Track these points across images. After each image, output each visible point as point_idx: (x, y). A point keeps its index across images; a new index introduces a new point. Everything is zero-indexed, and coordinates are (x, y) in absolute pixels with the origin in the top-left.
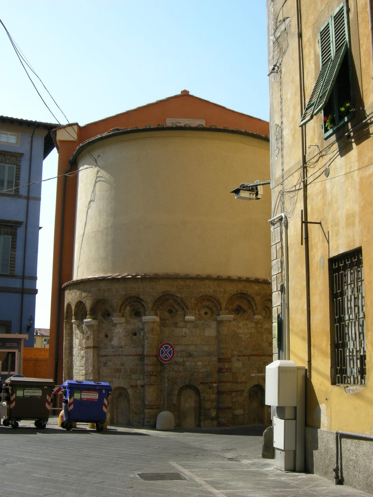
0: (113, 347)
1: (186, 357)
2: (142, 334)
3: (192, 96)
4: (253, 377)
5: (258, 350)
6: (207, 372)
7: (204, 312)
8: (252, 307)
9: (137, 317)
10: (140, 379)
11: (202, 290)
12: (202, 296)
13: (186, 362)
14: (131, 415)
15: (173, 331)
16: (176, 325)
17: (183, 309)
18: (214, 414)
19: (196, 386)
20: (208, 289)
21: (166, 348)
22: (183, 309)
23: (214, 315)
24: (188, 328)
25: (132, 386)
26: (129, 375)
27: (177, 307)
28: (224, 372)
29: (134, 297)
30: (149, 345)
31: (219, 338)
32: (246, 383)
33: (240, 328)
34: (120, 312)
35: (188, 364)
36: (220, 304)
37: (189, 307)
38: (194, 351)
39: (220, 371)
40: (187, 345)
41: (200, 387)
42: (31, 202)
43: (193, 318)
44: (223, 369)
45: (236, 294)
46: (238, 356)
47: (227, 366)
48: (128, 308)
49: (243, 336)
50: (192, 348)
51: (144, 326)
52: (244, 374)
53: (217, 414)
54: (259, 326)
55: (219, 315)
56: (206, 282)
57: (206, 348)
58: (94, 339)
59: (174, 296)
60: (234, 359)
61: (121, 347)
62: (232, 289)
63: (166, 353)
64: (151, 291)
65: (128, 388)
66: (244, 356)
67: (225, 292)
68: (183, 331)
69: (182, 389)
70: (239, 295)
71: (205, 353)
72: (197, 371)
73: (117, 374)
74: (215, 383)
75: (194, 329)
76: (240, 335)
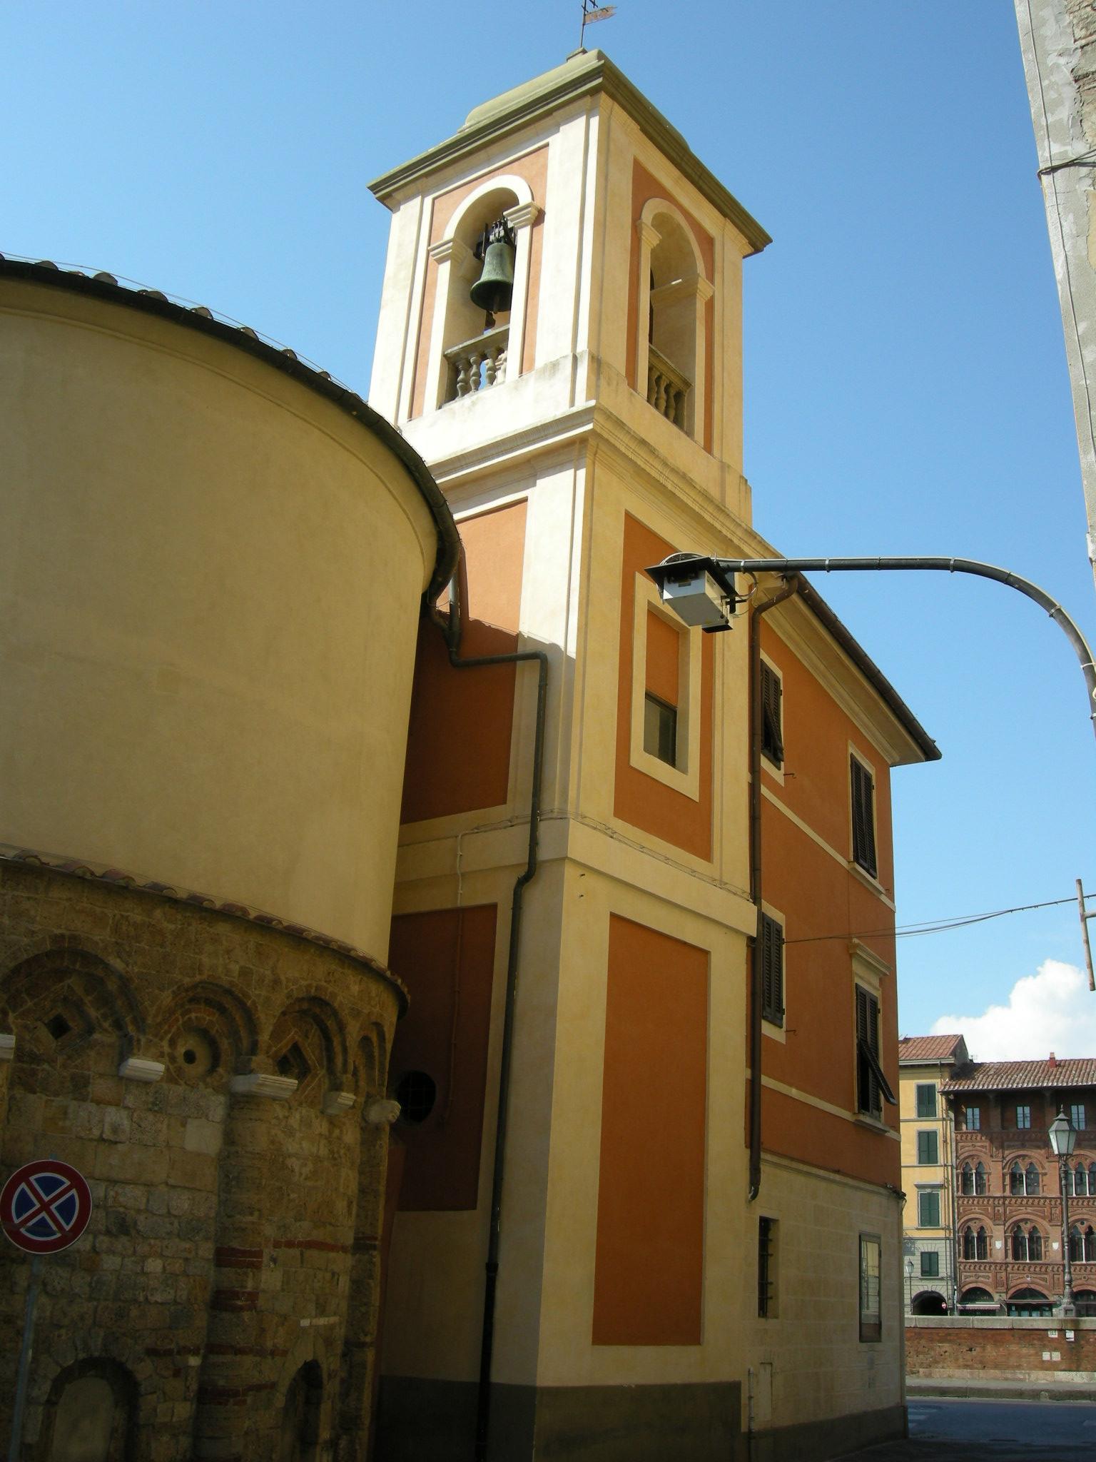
1: (108, 1232)
4: (304, 1329)
6: (176, 1302)
7: (183, 1050)
8: (331, 1060)
11: (205, 960)
12: (195, 986)
13: (104, 1256)
15: (66, 1113)
16: (79, 1087)
17: (118, 1025)
19: (129, 1366)
20: (226, 958)
21: (49, 1185)
22: (118, 1025)
23: (220, 1070)
24: (127, 1108)
27: (93, 1013)
28: (241, 1308)
31: (231, 1165)
32: (285, 1353)
33: (290, 1133)
35: (110, 1263)
36: (253, 1028)
37: (149, 1021)
38: (139, 1211)
39: (222, 1301)
40: (114, 1182)
41: (144, 1370)
43: (159, 1067)
44: (236, 1295)
46: (277, 1245)
47: (250, 1285)
50: (132, 1197)
52: (285, 1317)
55: (242, 1069)
56: (222, 928)
57: (182, 1203)
62: (298, 973)
63: (45, 1207)
66: (290, 1244)
67: (276, 982)
68: (108, 1119)
69: (66, 1376)
70: (305, 1006)
71: (176, 1224)
72: (141, 1299)
74: (195, 1352)
75: (151, 1117)
76: (289, 1162)
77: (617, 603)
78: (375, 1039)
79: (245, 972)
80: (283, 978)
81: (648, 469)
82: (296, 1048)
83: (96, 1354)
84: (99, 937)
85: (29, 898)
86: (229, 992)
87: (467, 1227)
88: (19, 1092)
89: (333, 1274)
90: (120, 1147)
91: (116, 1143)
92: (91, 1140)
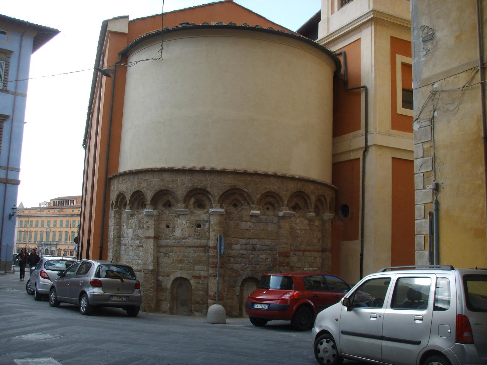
0: (175, 239)
2: (207, 226)
3: (236, 4)
5: (310, 245)
7: (266, 208)
9: (201, 209)
10: (203, 271)
12: (267, 192)
20: (274, 186)
24: (253, 222)
25: (195, 277)
26: (192, 266)
29: (200, 189)
33: (297, 224)
42: (19, 98)
43: (259, 212)
45: (296, 192)
48: (192, 200)
49: (299, 231)
51: (209, 218)
54: (312, 223)
58: (154, 229)
59: (241, 190)
60: (292, 254)
61: (184, 238)
64: (219, 184)
65: (191, 279)
66: (299, 251)
73: (180, 265)
76: (297, 231)
77: (389, 66)
78: (323, 199)
79: (278, 188)
81: (396, 22)
82: (296, 204)
83: (250, 276)
85: (223, 178)
86: (275, 193)
87: (356, 244)
88: (227, 221)
89: (314, 257)
91: (251, 230)
92: (245, 230)
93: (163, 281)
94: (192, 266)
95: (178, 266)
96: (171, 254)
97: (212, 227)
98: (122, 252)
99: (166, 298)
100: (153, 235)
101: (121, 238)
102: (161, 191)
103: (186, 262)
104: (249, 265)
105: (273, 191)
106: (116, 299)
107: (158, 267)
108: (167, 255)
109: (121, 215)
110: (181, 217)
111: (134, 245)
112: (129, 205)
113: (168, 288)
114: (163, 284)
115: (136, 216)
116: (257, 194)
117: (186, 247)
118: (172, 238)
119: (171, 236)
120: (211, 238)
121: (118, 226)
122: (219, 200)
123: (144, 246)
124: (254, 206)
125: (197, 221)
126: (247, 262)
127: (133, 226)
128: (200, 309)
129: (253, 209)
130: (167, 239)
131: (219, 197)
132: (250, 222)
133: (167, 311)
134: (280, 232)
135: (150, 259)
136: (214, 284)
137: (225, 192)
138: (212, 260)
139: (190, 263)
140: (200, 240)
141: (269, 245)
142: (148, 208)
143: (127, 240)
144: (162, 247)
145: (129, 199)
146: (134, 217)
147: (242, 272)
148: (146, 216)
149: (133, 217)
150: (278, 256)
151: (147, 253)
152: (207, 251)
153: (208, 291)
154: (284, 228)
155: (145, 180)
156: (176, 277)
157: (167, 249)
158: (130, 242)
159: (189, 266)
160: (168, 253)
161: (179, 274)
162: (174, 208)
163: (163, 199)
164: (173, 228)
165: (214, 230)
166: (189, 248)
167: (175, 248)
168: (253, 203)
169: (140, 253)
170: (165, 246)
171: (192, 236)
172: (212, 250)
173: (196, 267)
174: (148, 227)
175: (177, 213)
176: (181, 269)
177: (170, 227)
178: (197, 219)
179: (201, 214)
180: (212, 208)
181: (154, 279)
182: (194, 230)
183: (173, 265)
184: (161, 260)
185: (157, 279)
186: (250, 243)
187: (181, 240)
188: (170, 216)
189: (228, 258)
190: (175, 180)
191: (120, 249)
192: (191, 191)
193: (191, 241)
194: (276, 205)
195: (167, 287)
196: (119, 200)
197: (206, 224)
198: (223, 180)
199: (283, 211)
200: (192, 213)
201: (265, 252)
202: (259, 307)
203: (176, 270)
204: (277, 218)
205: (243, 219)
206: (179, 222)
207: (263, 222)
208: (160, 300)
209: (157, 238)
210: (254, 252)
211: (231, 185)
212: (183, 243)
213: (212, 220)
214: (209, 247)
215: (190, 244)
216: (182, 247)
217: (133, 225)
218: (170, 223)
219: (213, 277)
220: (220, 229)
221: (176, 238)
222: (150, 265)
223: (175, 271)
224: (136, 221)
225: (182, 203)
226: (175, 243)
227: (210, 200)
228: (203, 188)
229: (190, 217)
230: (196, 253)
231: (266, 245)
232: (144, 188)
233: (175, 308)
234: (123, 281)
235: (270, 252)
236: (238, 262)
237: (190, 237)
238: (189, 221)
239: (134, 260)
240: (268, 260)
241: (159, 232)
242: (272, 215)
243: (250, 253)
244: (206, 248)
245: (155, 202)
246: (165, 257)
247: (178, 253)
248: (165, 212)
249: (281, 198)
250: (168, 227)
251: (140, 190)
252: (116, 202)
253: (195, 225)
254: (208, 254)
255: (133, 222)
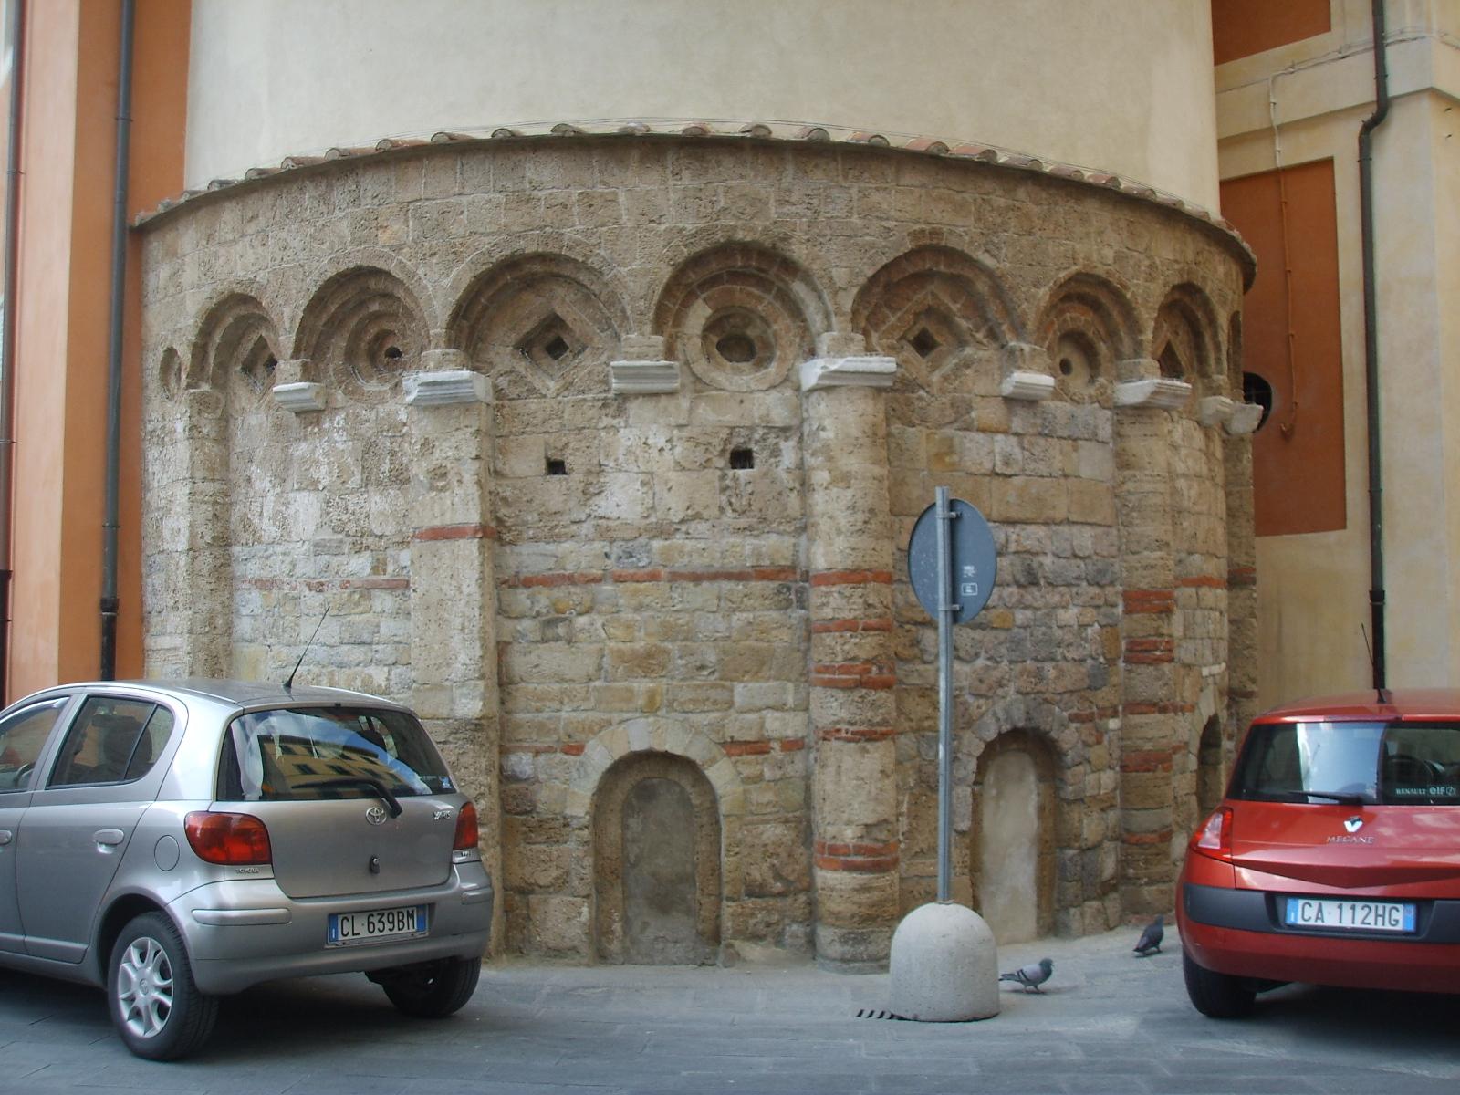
0: (605, 533)
2: (789, 456)
9: (744, 366)
10: (781, 708)
14: (728, 908)
18: (1109, 866)
19: (1054, 734)
24: (1016, 434)
25: (733, 747)
26: (713, 686)
29: (746, 249)
30: (860, 517)
34: (658, 330)
41: (1069, 738)
48: (699, 314)
53: (1124, 863)
56: (1091, 206)
58: (479, 483)
61: (663, 531)
64: (855, 219)
65: (713, 761)
68: (997, 450)
74: (1115, 715)
79: (1119, 258)
80: (1158, 262)
83: (1021, 724)
84: (961, 230)
85: (877, 189)
86: (1104, 284)
87: (1340, 552)
88: (896, 428)
90: (1015, 480)
91: (1010, 476)
92: (984, 475)
93: (542, 777)
94: (713, 686)
95: (630, 690)
96: (582, 621)
97: (830, 459)
98: (244, 626)
99: (567, 873)
100: (472, 515)
101: (236, 550)
102: (512, 263)
103: (681, 662)
104: (1011, 662)
105: (1101, 271)
106: (364, 934)
107: (502, 702)
108: (561, 630)
109: (225, 421)
110: (634, 407)
111: (338, 580)
112: (292, 357)
113: (573, 817)
114: (544, 798)
115: (340, 418)
116: (1037, 284)
117: (675, 577)
118: (586, 528)
119: (580, 522)
120: (824, 525)
121: (213, 480)
122: (855, 312)
123: (420, 581)
124: (1027, 348)
125: (733, 428)
126: (1003, 650)
127: (323, 474)
128: (768, 925)
129: (1013, 359)
130: (556, 538)
131: (855, 291)
132: (1005, 432)
133: (575, 949)
134: (1130, 486)
135: (463, 658)
136: (858, 778)
137: (885, 267)
138: (836, 648)
139: (702, 667)
140: (756, 536)
141: (1089, 557)
142: (432, 364)
143: (284, 554)
144: (528, 583)
145: (292, 320)
146: (326, 426)
147: (982, 701)
148: (425, 409)
149: (318, 423)
150: (1120, 610)
151: (442, 622)
152: (793, 597)
153: (809, 821)
154: (1149, 463)
155: (404, 207)
156: (620, 751)
157: (558, 592)
158: (307, 569)
159: (699, 686)
160: (566, 619)
161: (639, 735)
162: (588, 362)
163: (524, 307)
164: (589, 472)
165: (843, 479)
166: (691, 585)
167: (608, 588)
168: (1019, 329)
169: (378, 626)
170: (548, 581)
171: (705, 515)
172: (834, 589)
173: (739, 688)
174: (440, 474)
175: (615, 384)
176: (651, 707)
177: (567, 466)
178: (731, 418)
179: (752, 392)
180: (812, 353)
181: (488, 772)
182: (717, 484)
183: (597, 683)
184: (520, 663)
185: (501, 769)
186: (1013, 547)
187: (643, 540)
188: (568, 409)
189: (908, 631)
190: (602, 195)
191: (229, 610)
192: (696, 261)
193: (697, 548)
194: (1103, 348)
195: (568, 812)
196: (217, 338)
197: (783, 445)
198: (876, 197)
199: (1141, 378)
200: (700, 386)
201: (1074, 590)
202: (1347, 923)
203: (622, 711)
204: (1108, 413)
205: (973, 414)
206: (627, 437)
207: (1059, 434)
208: (526, 890)
209: (494, 533)
210: (1033, 595)
211: (917, 227)
212: (657, 559)
213: (826, 423)
214: (806, 576)
215: (698, 563)
216: (653, 577)
217: (324, 469)
218: (567, 444)
219: (849, 740)
220: (877, 471)
221: (608, 529)
222: (465, 690)
223: (616, 717)
224: (340, 446)
225: (648, 328)
226: (607, 555)
227: (796, 311)
228: (768, 244)
229: (691, 410)
230: (734, 611)
231: (1075, 556)
232: (398, 248)
233: (617, 927)
234: (395, 811)
235: (1095, 590)
236: (962, 654)
237: (693, 524)
238: (685, 434)
239: (341, 666)
240: (1089, 631)
241: (505, 500)
242: (1090, 397)
243: (1014, 600)
244: (789, 581)
245: (470, 327)
246: (544, 641)
247: (627, 615)
248: (538, 385)
249: (1128, 311)
250: (556, 467)
251: (380, 264)
252: (200, 350)
253: (723, 451)
254: (803, 611)
255: (319, 451)
